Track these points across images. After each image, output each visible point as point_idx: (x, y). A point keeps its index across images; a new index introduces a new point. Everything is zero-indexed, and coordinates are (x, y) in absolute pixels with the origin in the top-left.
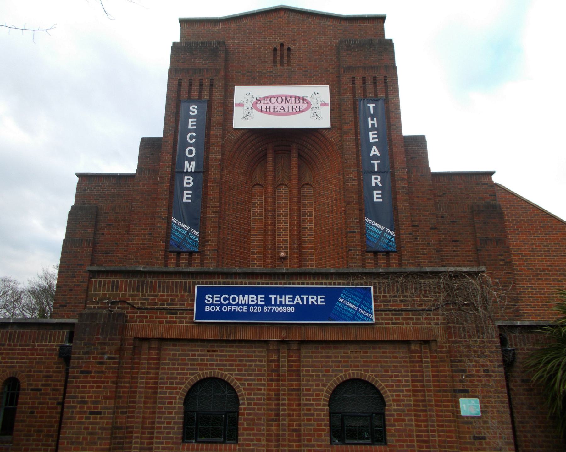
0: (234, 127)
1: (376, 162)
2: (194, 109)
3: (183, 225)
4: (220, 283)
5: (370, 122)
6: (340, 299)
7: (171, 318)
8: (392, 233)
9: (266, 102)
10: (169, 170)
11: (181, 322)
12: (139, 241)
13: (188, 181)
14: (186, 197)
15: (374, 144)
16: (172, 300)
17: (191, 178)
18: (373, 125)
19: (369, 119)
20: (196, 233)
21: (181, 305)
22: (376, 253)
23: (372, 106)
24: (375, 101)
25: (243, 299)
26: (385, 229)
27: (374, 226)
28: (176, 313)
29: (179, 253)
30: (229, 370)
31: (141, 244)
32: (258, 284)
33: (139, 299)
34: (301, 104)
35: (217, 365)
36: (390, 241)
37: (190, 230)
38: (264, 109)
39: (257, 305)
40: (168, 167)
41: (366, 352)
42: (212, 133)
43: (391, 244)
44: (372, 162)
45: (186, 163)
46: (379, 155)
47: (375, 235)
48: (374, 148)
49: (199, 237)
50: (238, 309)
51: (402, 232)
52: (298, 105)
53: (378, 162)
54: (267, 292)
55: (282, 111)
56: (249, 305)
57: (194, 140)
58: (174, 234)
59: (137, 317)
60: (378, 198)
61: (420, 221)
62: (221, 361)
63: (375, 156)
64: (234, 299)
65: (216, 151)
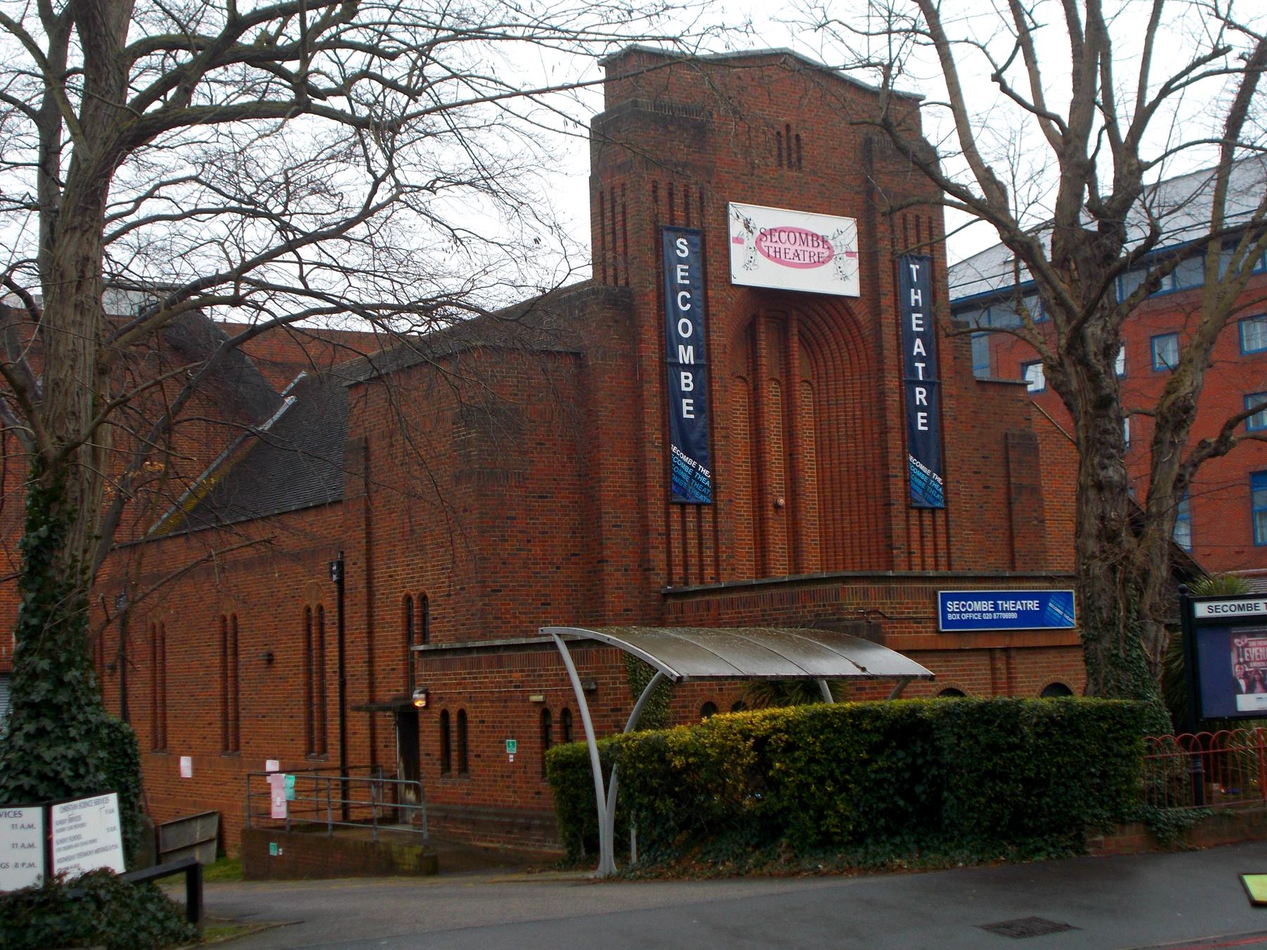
0: (734, 281)
1: (920, 366)
2: (682, 247)
4: (954, 589)
6: (1051, 605)
7: (917, 627)
8: (939, 480)
9: (774, 240)
10: (655, 357)
11: (926, 632)
12: (617, 482)
13: (686, 381)
14: (687, 406)
15: (919, 335)
16: (917, 608)
17: (689, 375)
18: (916, 301)
19: (913, 290)
20: (706, 472)
21: (925, 613)
22: (921, 510)
23: (914, 267)
24: (920, 259)
25: (977, 606)
26: (931, 474)
27: (918, 469)
28: (920, 623)
29: (683, 506)
30: (961, 680)
31: (620, 487)
32: (985, 589)
33: (889, 608)
34: (820, 249)
35: (953, 676)
36: (938, 492)
37: (697, 467)
38: (772, 254)
39: (988, 612)
40: (654, 353)
41: (1062, 657)
42: (710, 293)
43: (938, 496)
44: (917, 364)
45: (681, 348)
46: (924, 354)
47: (920, 483)
48: (918, 342)
50: (974, 616)
51: (950, 478)
52: (816, 251)
53: (923, 365)
54: (994, 597)
55: (796, 260)
56: (982, 612)
57: (688, 306)
58: (677, 474)
59: (889, 628)
60: (923, 425)
61: (963, 461)
62: (956, 671)
63: (919, 354)
64: (970, 606)
65: (718, 328)
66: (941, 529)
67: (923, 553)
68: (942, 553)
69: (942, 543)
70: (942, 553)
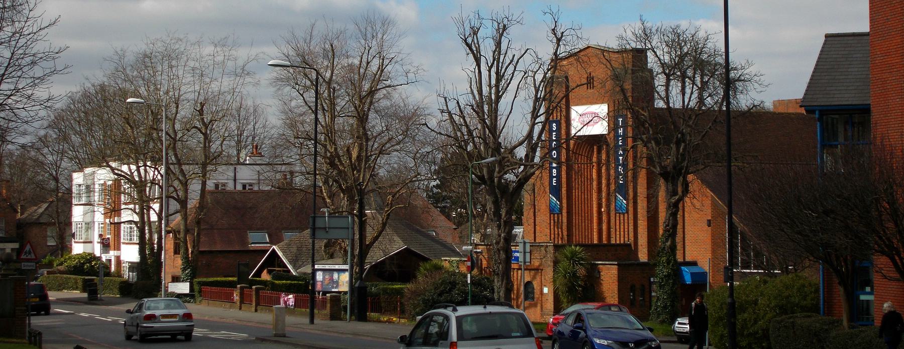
1: (621, 158)
3: (554, 199)
5: (620, 131)
8: (625, 202)
13: (554, 171)
17: (555, 170)
20: (558, 203)
22: (620, 213)
29: (554, 214)
49: (560, 205)
66: (626, 221)
67: (620, 230)
68: (626, 230)
69: (626, 227)
70: (626, 230)
